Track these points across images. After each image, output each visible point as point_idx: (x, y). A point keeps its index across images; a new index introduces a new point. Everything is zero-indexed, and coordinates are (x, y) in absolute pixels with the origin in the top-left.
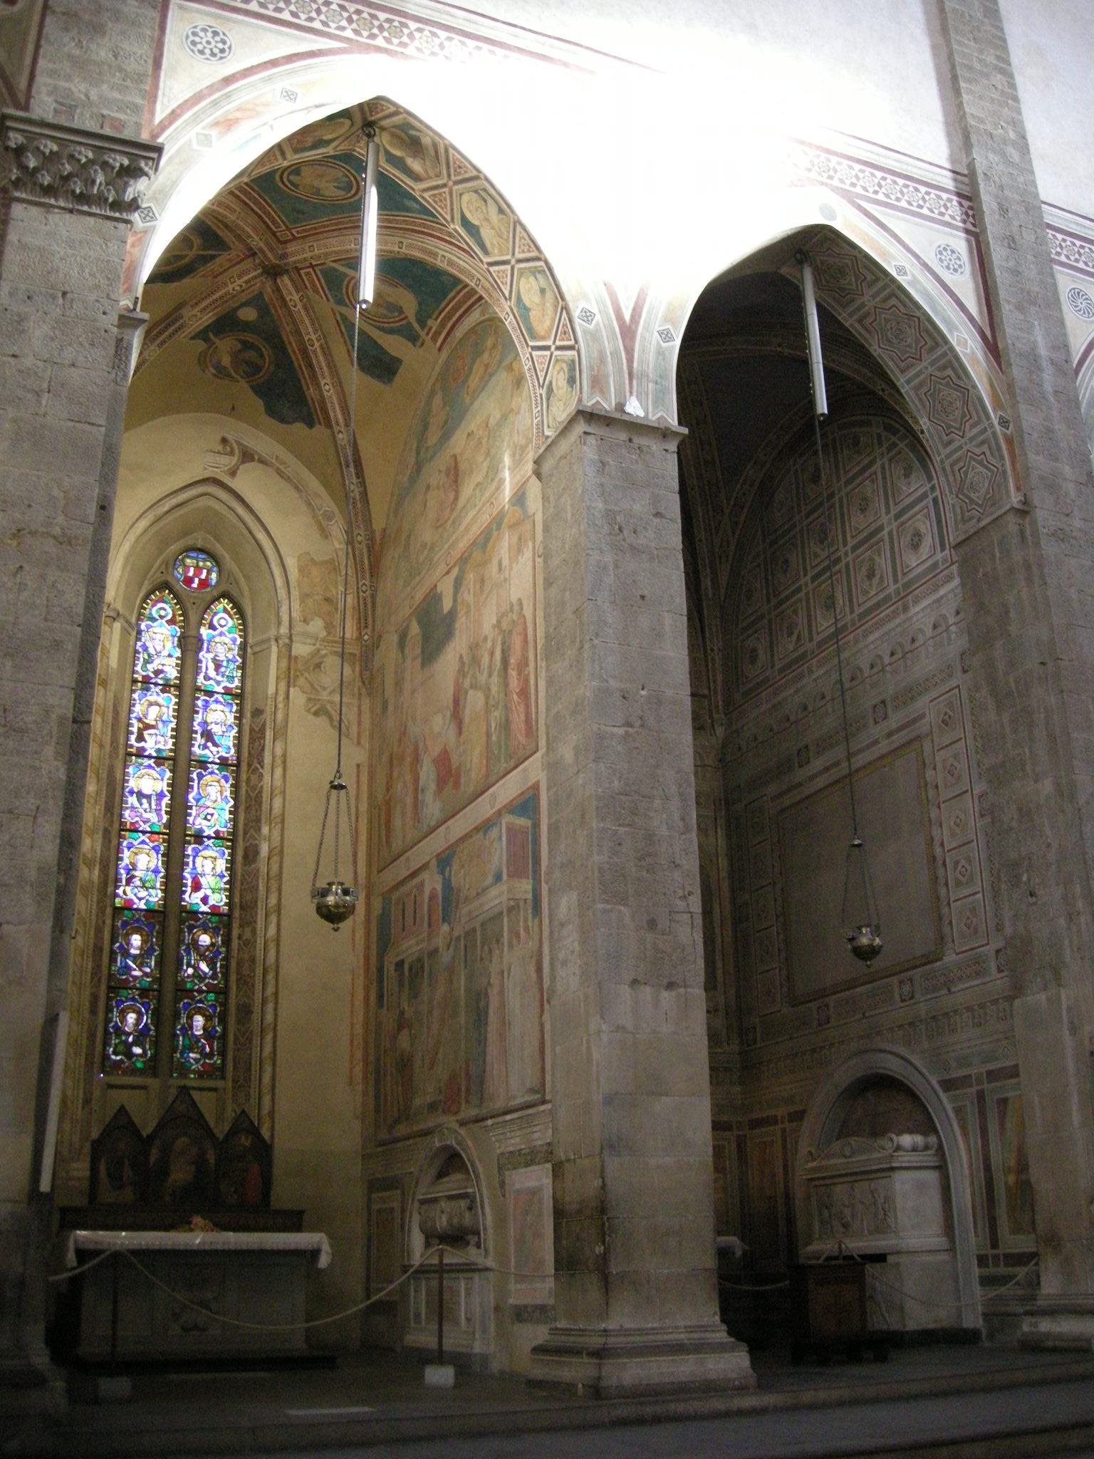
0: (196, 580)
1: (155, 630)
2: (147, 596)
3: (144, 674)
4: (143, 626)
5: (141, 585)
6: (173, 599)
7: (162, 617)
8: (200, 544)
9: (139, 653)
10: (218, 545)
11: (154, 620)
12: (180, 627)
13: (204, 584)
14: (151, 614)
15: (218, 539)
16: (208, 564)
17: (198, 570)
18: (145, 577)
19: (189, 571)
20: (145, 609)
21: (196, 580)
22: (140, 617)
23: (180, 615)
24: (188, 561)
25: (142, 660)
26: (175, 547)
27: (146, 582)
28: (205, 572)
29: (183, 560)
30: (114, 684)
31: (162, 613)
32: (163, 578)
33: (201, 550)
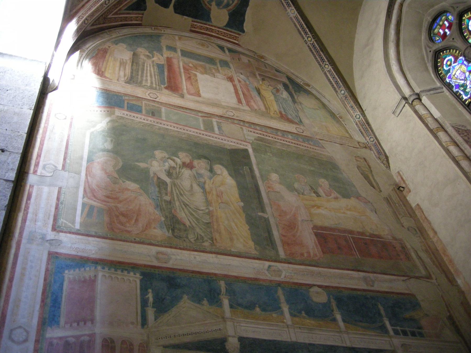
0: (447, 30)
1: (453, 74)
2: (436, 68)
3: (469, 96)
4: (448, 80)
5: (427, 69)
6: (446, 52)
7: (450, 65)
8: (430, 19)
9: (458, 92)
10: (436, 7)
11: (449, 71)
12: (461, 56)
13: (449, 28)
14: (445, 70)
15: (432, 6)
16: (443, 18)
17: (443, 27)
18: (425, 64)
19: (440, 33)
20: (441, 73)
21: (447, 30)
22: (442, 80)
23: (456, 52)
24: (436, 31)
25: (462, 93)
26: (424, 36)
27: (428, 65)
28: (446, 23)
29: (434, 34)
30: (446, 122)
31: (449, 63)
32: (432, 52)
33: (434, 20)
